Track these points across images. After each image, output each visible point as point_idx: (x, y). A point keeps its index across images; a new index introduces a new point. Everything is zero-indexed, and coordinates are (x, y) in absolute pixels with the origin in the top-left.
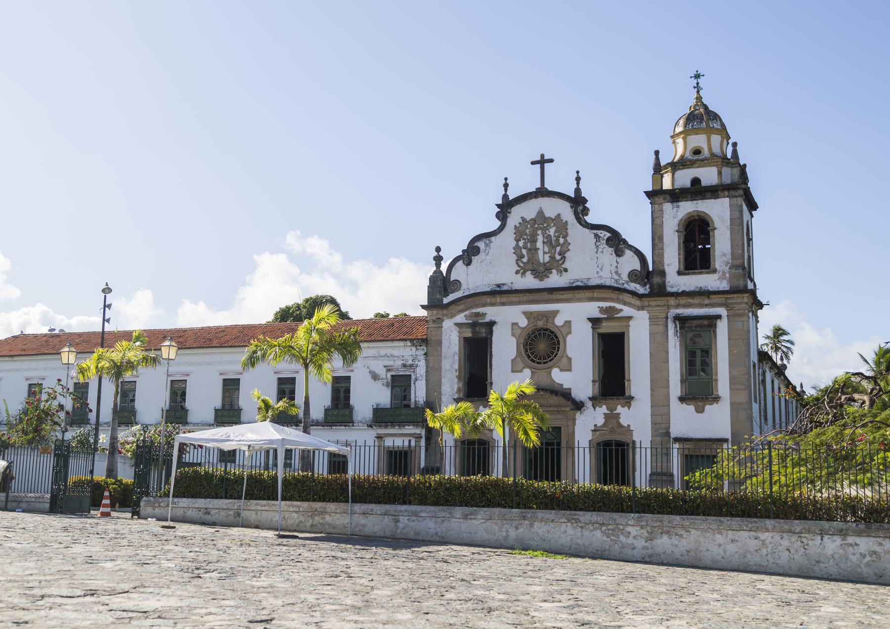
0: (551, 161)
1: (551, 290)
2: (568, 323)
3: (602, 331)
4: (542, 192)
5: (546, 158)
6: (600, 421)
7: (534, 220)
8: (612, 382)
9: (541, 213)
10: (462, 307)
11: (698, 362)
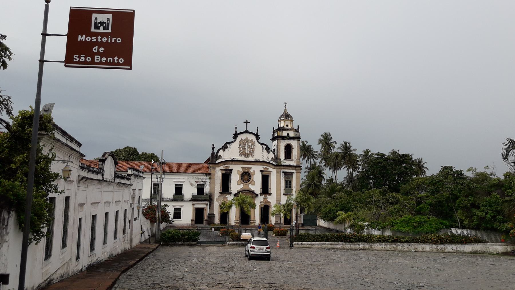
2: (254, 171)
4: (247, 132)
6: (262, 200)
8: (265, 189)
9: (247, 138)
11: (288, 185)
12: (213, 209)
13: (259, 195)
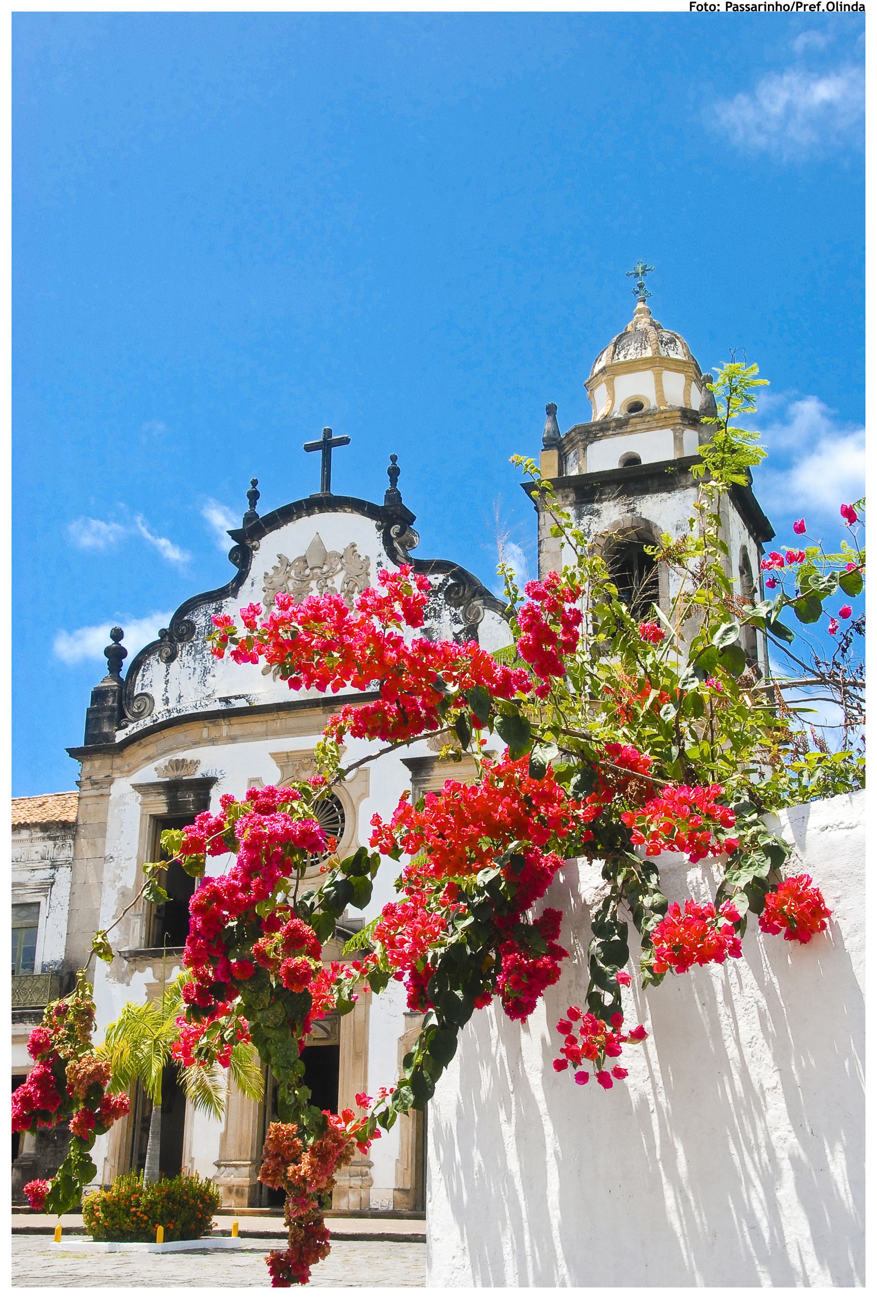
0: (345, 441)
9: (317, 544)
10: (150, 750)
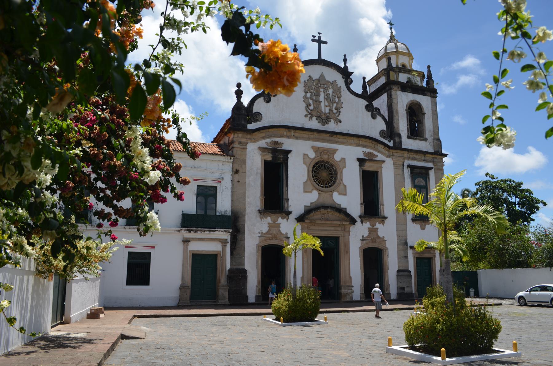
0: (326, 43)
1: (334, 133)
2: (343, 160)
3: (366, 168)
5: (322, 39)
6: (366, 234)
7: (319, 80)
9: (322, 76)
10: (263, 135)
12: (242, 256)
13: (359, 220)
